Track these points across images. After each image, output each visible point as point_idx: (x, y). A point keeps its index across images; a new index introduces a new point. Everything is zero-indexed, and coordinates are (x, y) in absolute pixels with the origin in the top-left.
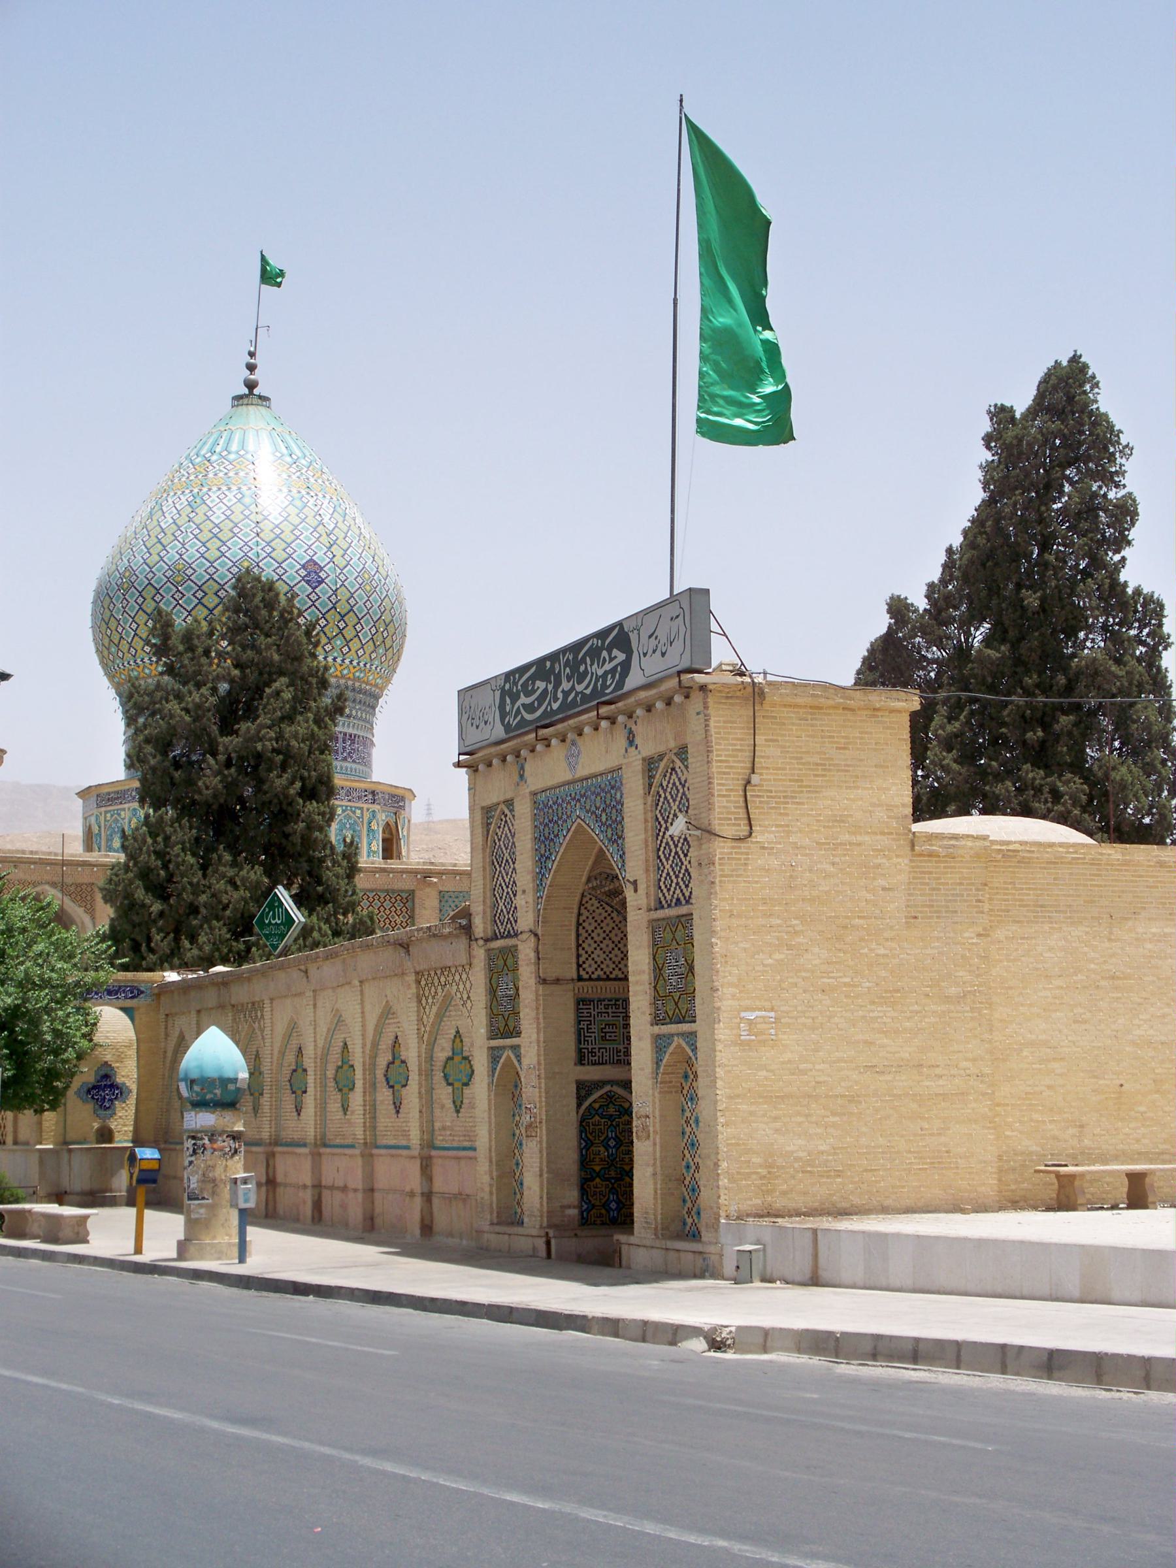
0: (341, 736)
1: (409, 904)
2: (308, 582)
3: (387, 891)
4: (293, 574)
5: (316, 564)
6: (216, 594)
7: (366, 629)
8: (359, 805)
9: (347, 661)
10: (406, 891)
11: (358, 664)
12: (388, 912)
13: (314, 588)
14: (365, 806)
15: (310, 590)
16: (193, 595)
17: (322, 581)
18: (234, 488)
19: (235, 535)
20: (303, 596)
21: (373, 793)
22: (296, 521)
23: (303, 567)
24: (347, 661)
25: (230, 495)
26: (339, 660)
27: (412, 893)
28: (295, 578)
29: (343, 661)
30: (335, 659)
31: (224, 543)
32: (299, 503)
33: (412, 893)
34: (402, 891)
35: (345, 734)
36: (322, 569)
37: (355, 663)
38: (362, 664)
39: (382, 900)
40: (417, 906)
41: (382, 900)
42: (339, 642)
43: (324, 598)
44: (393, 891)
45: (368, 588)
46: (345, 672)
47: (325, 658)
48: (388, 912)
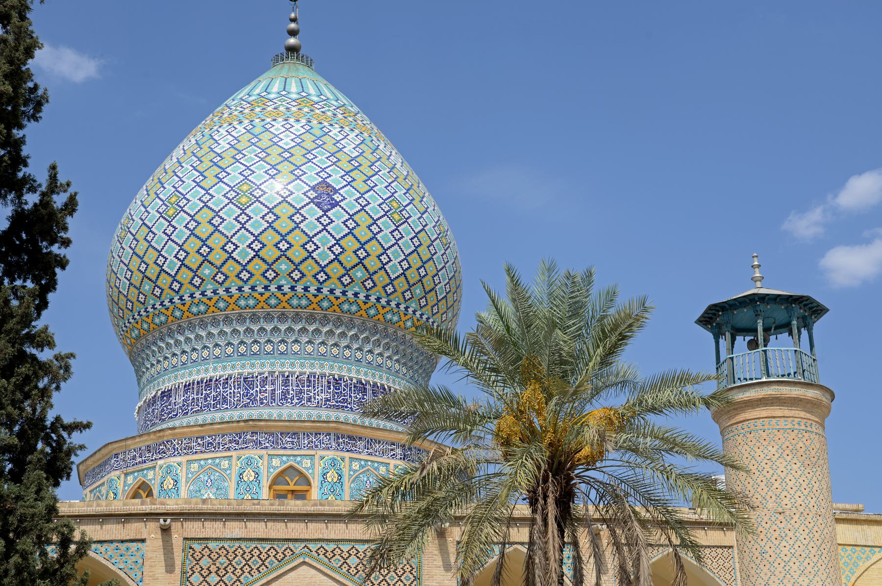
2: (318, 205)
5: (329, 186)
6: (210, 222)
7: (395, 262)
8: (384, 459)
9: (373, 299)
11: (388, 303)
13: (325, 211)
14: (393, 462)
15: (321, 213)
16: (186, 227)
17: (337, 204)
18: (246, 122)
19: (238, 161)
20: (312, 219)
22: (309, 145)
23: (313, 188)
24: (373, 299)
25: (240, 128)
26: (362, 296)
28: (302, 200)
29: (367, 297)
30: (356, 295)
31: (215, 164)
32: (319, 133)
35: (375, 385)
36: (336, 191)
37: (383, 301)
38: (393, 304)
43: (338, 222)
45: (396, 217)
46: (372, 312)
47: (344, 293)
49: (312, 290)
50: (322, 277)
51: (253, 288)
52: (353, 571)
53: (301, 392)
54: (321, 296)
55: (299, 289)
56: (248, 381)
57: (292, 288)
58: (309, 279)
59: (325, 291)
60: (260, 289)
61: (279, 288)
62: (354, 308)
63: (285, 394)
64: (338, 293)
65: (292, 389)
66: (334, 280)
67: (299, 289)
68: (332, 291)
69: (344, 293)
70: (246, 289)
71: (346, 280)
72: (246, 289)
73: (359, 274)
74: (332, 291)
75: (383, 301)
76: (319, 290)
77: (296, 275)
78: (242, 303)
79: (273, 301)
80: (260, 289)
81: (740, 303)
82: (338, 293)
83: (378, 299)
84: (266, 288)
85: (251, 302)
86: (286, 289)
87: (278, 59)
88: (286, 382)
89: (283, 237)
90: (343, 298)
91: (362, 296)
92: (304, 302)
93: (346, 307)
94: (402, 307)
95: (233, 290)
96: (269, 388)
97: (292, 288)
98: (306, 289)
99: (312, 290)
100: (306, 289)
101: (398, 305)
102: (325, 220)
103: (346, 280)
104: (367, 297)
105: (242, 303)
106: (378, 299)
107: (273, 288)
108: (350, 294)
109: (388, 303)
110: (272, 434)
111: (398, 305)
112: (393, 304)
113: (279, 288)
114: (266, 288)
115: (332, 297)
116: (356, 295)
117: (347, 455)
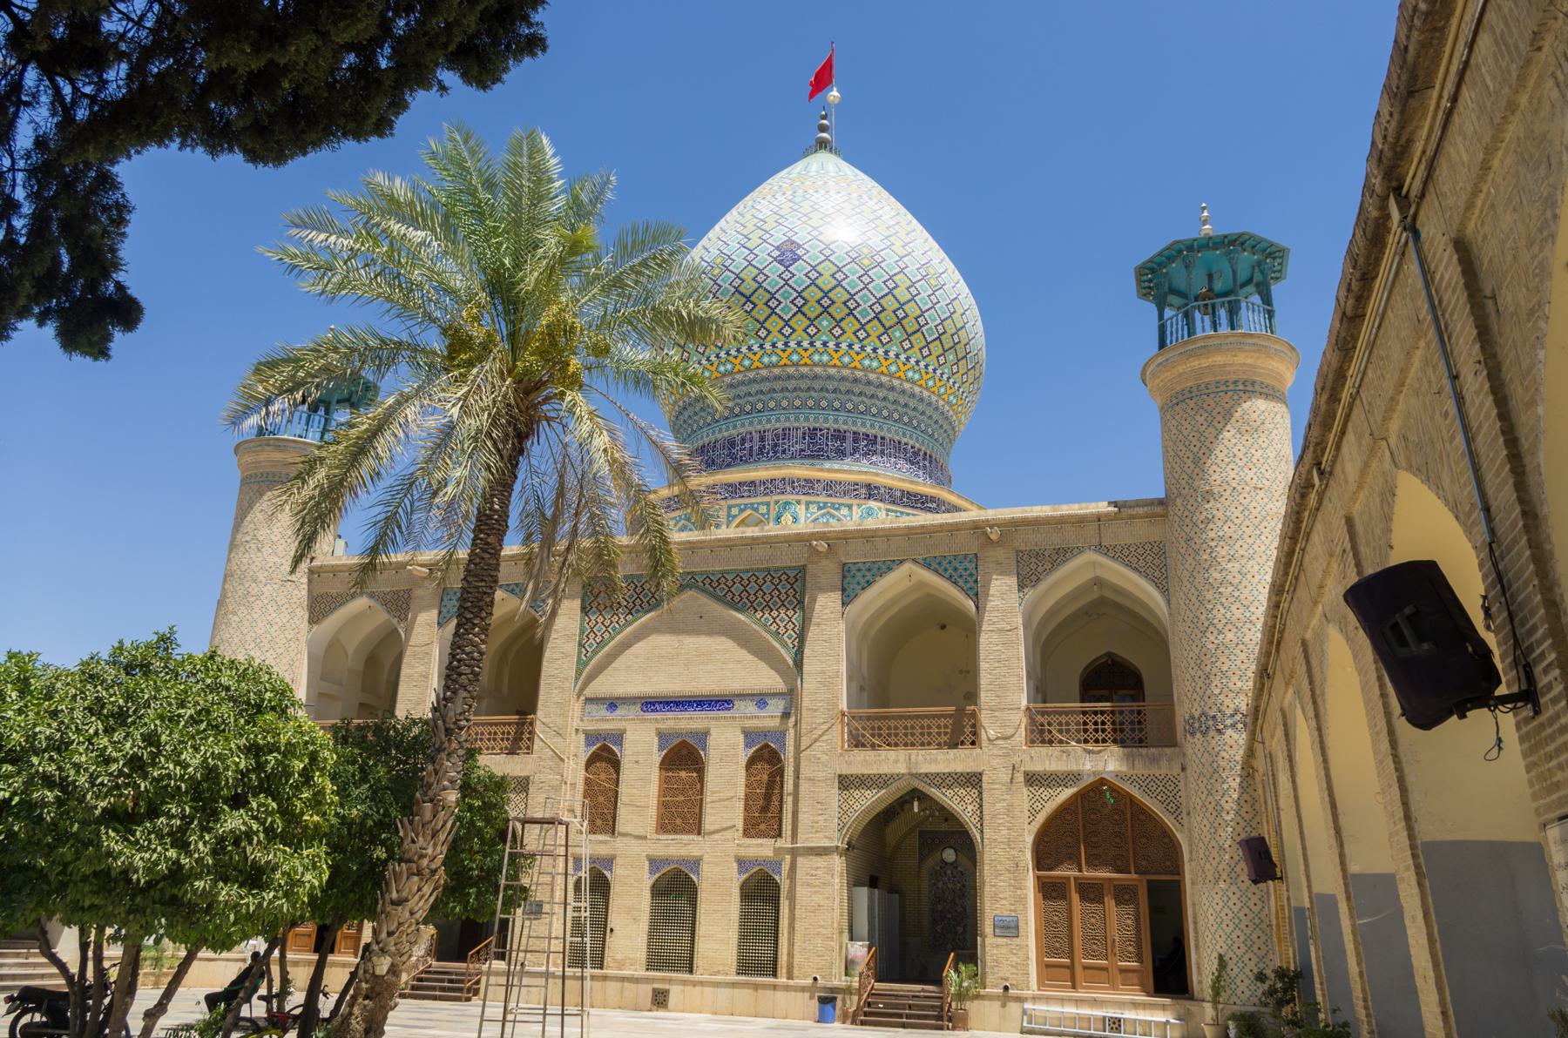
0: (850, 437)
1: (797, 586)
2: (780, 262)
3: (768, 570)
4: (764, 256)
5: (793, 242)
9: (844, 346)
10: (794, 568)
11: (862, 348)
12: (767, 597)
17: (800, 258)
21: (868, 486)
23: (778, 248)
26: (831, 345)
27: (802, 570)
29: (837, 345)
30: (825, 344)
33: (802, 570)
34: (790, 568)
36: (800, 246)
37: (857, 347)
38: (869, 349)
39: (761, 581)
40: (808, 585)
41: (761, 581)
42: (825, 323)
44: (777, 570)
46: (846, 360)
47: (812, 344)
48: (767, 597)
49: (780, 345)
50: (787, 331)
51: (728, 354)
52: (737, 599)
53: (776, 445)
54: (789, 350)
55: (768, 346)
56: (732, 443)
57: (761, 346)
58: (775, 336)
59: (792, 344)
60: (733, 352)
61: (750, 349)
62: (825, 358)
63: (761, 449)
64: (805, 344)
65: (768, 443)
66: (800, 331)
67: (768, 346)
68: (799, 344)
69: (812, 344)
70: (722, 354)
71: (812, 330)
72: (722, 354)
73: (825, 323)
74: (799, 344)
75: (857, 347)
76: (786, 344)
77: (763, 333)
78: (722, 369)
79: (747, 363)
80: (733, 352)
81: (1168, 258)
82: (805, 344)
83: (850, 346)
84: (738, 350)
85: (729, 367)
86: (755, 348)
87: (806, 153)
88: (762, 439)
89: (748, 299)
90: (812, 350)
91: (831, 345)
92: (774, 359)
93: (816, 358)
94: (881, 351)
95: (713, 358)
96: (747, 445)
97: (761, 346)
98: (774, 345)
99: (780, 345)
100: (774, 345)
101: (874, 350)
102: (786, 276)
103: (812, 330)
104: (837, 345)
105: (722, 369)
106: (850, 346)
107: (744, 349)
108: (818, 344)
109: (862, 348)
110: (730, 485)
111: (874, 350)
112: (869, 349)
113: (750, 349)
114: (738, 350)
115: (800, 350)
116: (825, 344)
117: (804, 498)
